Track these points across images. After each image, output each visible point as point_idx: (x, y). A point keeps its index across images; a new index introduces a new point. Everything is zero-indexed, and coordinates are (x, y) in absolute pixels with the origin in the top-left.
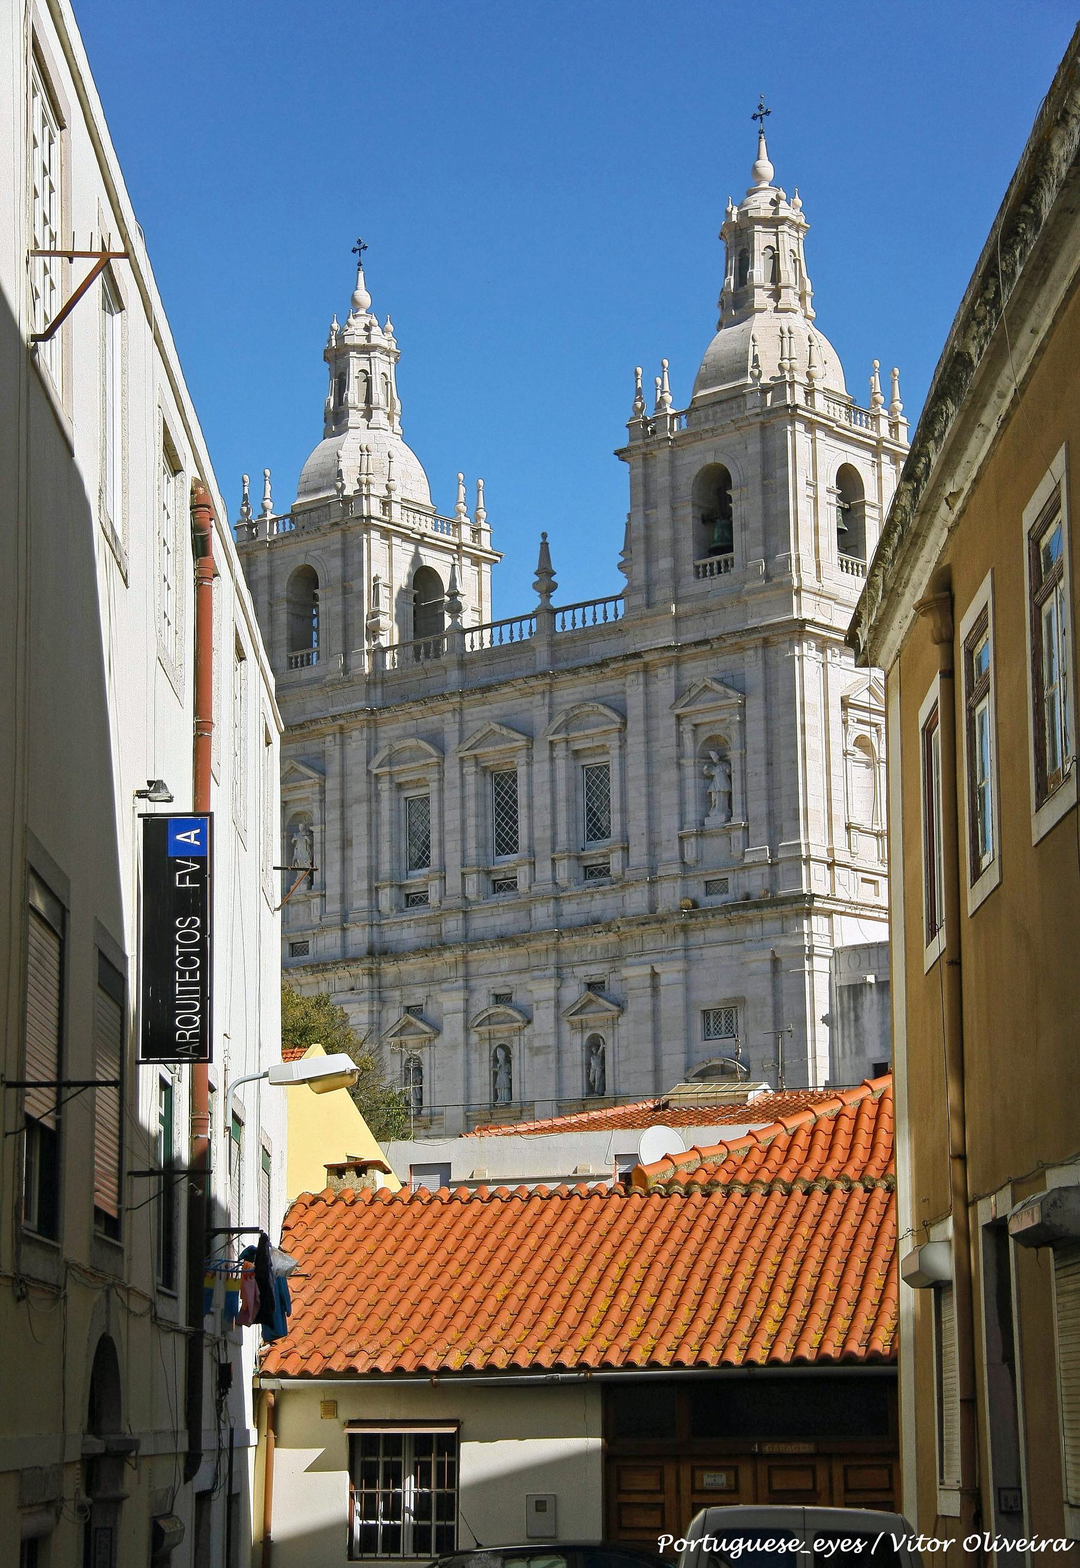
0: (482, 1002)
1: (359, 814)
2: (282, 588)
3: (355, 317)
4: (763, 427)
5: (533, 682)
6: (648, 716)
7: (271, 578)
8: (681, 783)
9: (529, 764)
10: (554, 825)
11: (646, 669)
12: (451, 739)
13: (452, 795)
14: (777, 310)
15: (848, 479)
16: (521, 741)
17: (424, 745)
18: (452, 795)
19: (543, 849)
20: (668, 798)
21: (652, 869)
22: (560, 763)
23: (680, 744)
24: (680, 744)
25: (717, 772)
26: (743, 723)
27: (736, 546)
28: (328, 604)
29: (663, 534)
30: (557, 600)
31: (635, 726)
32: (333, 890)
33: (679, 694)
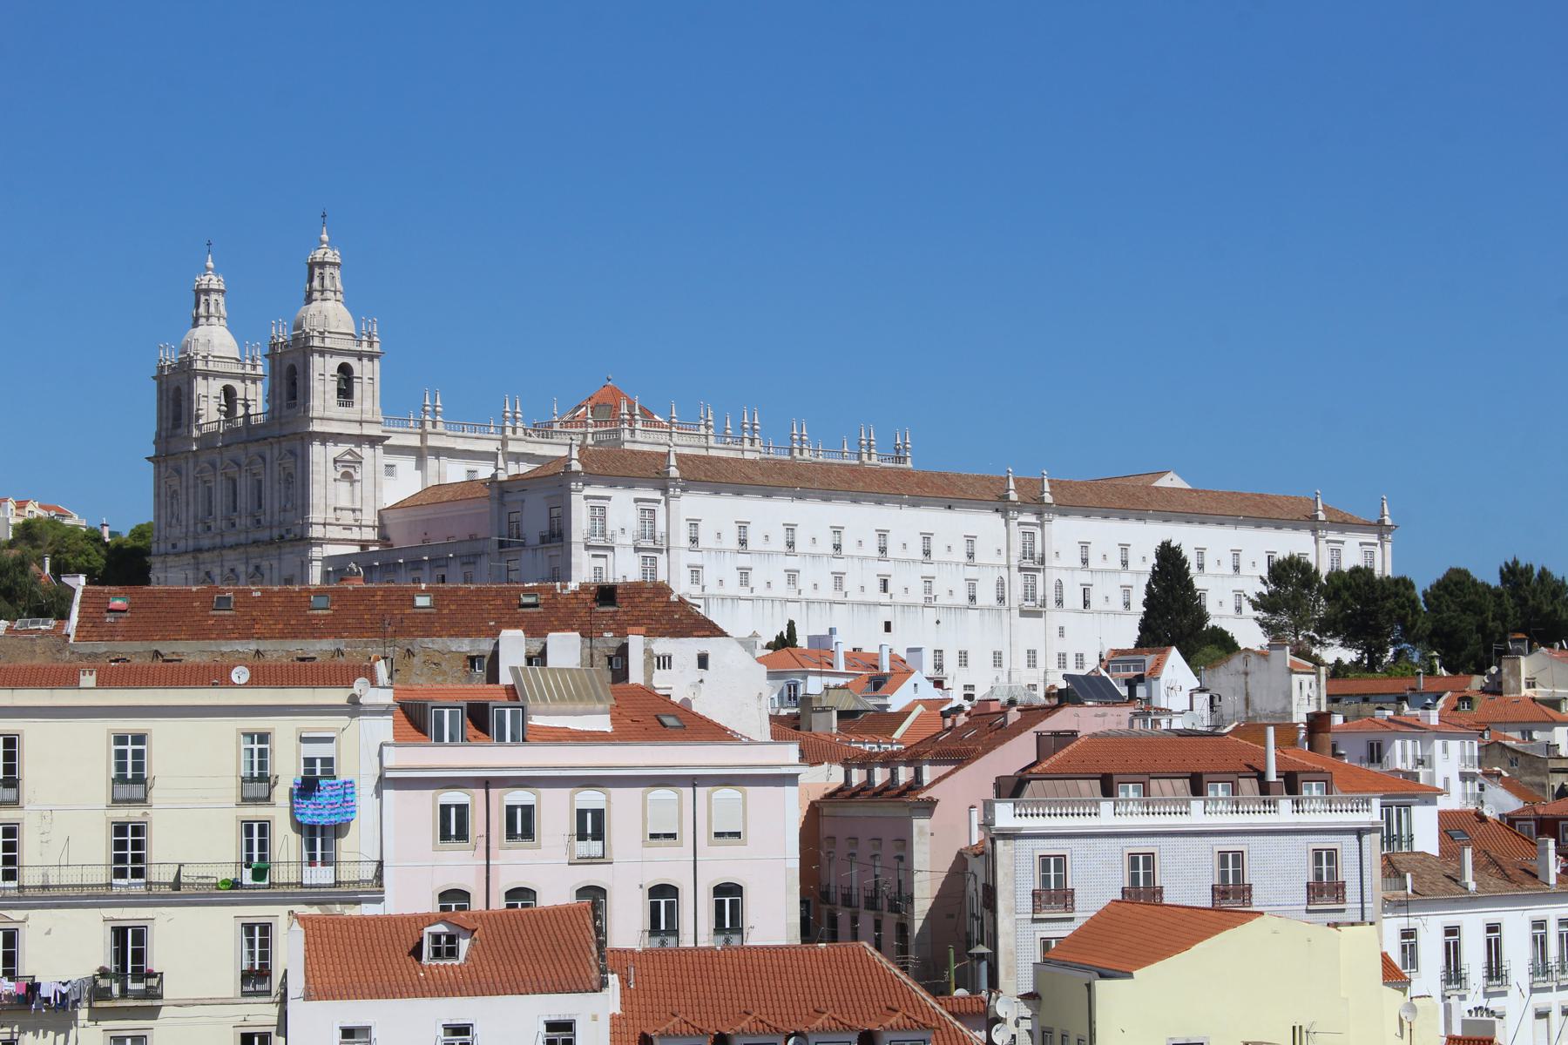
0: (226, 570)
1: (191, 491)
2: (171, 394)
3: (205, 275)
4: (304, 352)
5: (240, 445)
6: (272, 462)
7: (167, 390)
8: (280, 488)
9: (240, 477)
10: (246, 503)
11: (271, 443)
12: (218, 464)
13: (219, 487)
14: (322, 300)
15: (345, 370)
16: (237, 469)
17: (210, 468)
18: (219, 487)
19: (243, 511)
20: (276, 495)
21: (271, 522)
22: (249, 478)
23: (280, 474)
24: (280, 474)
25: (291, 486)
26: (296, 468)
27: (298, 397)
28: (184, 404)
29: (278, 390)
30: (252, 411)
31: (268, 466)
32: (184, 523)
33: (280, 454)
